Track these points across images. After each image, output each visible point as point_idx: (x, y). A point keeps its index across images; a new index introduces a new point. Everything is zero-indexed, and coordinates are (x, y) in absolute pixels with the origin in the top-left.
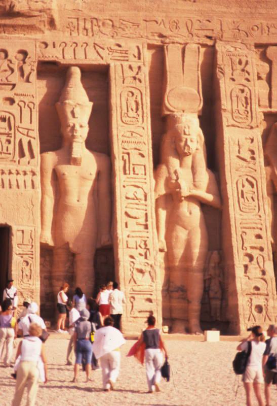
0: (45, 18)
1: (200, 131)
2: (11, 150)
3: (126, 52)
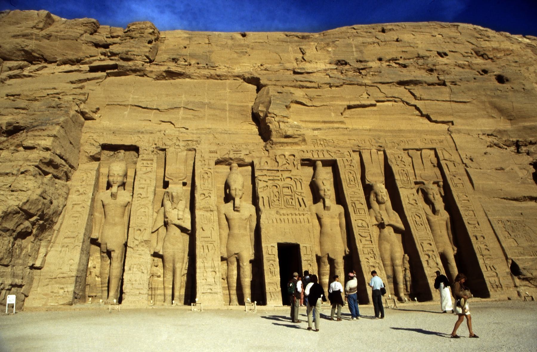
0: (301, 138)
1: (386, 190)
2: (293, 203)
3: (343, 154)
